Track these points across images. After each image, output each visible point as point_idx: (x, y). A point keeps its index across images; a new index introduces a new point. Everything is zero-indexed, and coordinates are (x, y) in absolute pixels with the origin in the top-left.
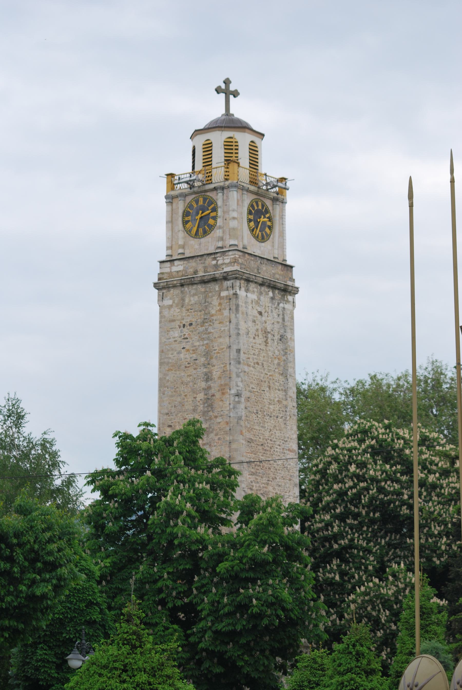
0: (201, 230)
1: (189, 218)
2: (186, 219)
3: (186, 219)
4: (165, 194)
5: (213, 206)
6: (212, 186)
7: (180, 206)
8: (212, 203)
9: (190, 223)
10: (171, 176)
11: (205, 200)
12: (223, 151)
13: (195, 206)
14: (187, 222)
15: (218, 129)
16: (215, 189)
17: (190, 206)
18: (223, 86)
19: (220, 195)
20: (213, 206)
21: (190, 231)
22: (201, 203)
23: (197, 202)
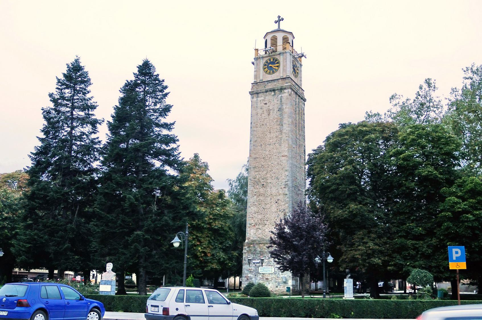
0: (271, 71)
1: (266, 67)
2: (265, 67)
3: (265, 67)
4: (254, 57)
5: (277, 61)
6: (278, 53)
7: (262, 62)
8: (277, 60)
9: (267, 69)
10: (257, 50)
11: (273, 59)
12: (282, 41)
13: (269, 62)
14: (265, 68)
15: (280, 31)
16: (280, 54)
17: (267, 62)
18: (281, 18)
19: (281, 56)
20: (277, 61)
21: (267, 72)
22: (272, 60)
23: (270, 60)
